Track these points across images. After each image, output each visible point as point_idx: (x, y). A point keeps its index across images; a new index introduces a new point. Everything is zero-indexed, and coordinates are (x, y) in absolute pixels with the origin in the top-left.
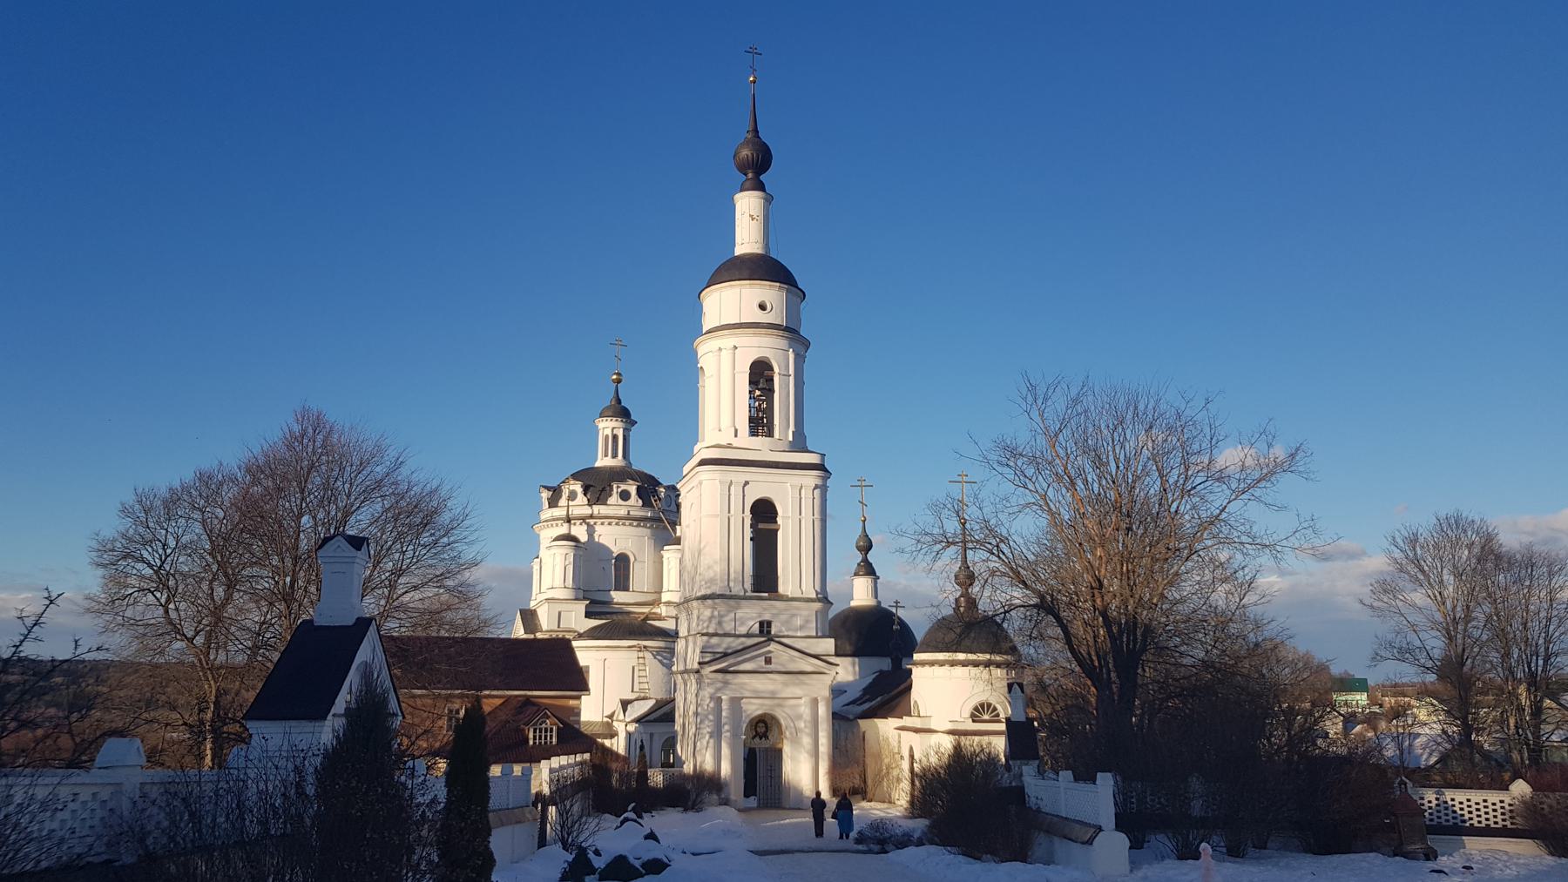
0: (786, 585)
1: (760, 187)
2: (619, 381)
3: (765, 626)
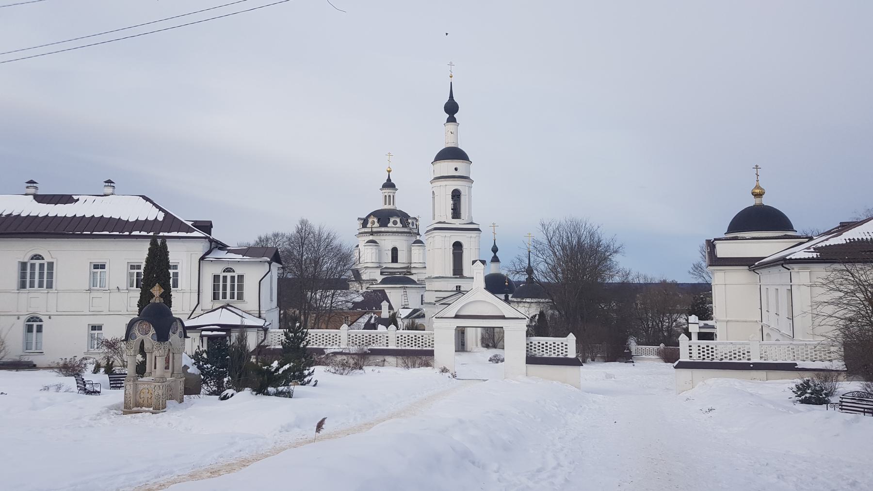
0: (465, 274)
2: (389, 172)
3: (458, 288)
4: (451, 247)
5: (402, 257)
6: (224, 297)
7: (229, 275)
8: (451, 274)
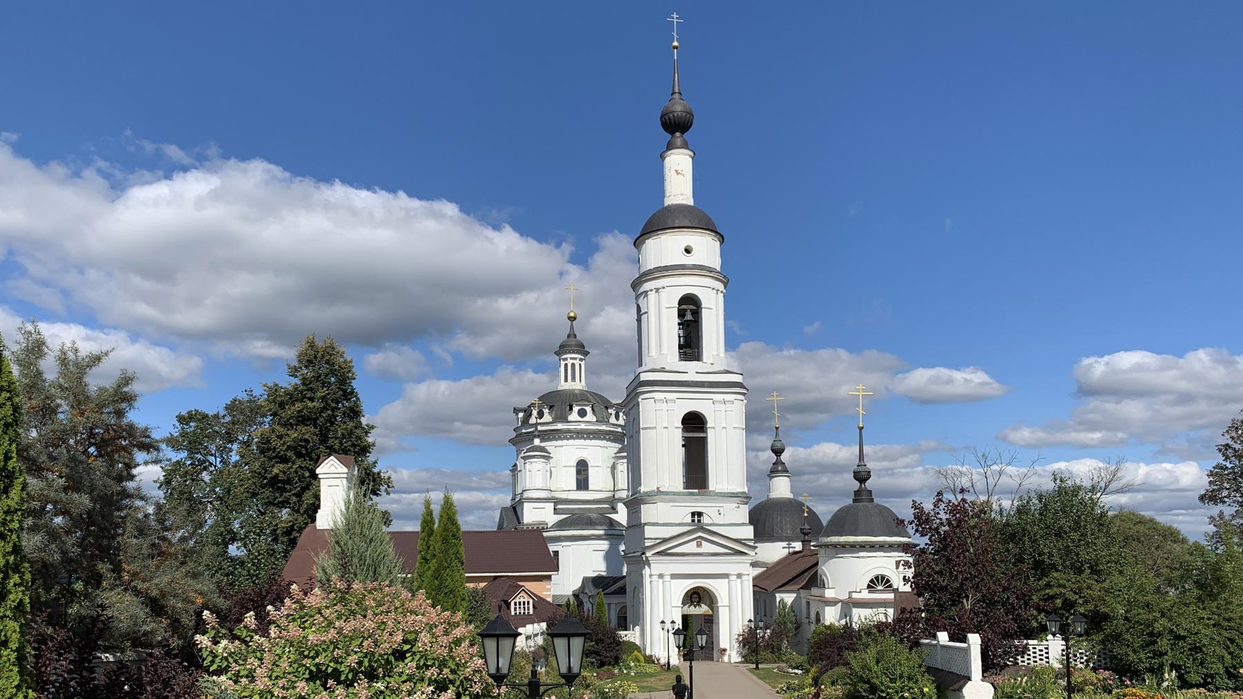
0: (716, 482)
4: (680, 425)
5: (600, 482)
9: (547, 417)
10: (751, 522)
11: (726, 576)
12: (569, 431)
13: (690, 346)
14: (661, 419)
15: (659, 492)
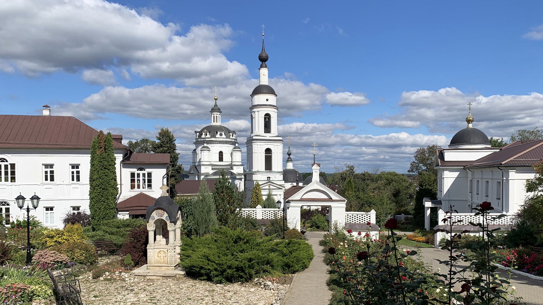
0: (274, 169)
1: (266, 67)
5: (227, 158)
6: (139, 187)
7: (141, 173)
8: (264, 169)
9: (208, 136)
10: (284, 180)
11: (276, 195)
12: (216, 141)
13: (267, 128)
14: (259, 150)
15: (258, 171)
